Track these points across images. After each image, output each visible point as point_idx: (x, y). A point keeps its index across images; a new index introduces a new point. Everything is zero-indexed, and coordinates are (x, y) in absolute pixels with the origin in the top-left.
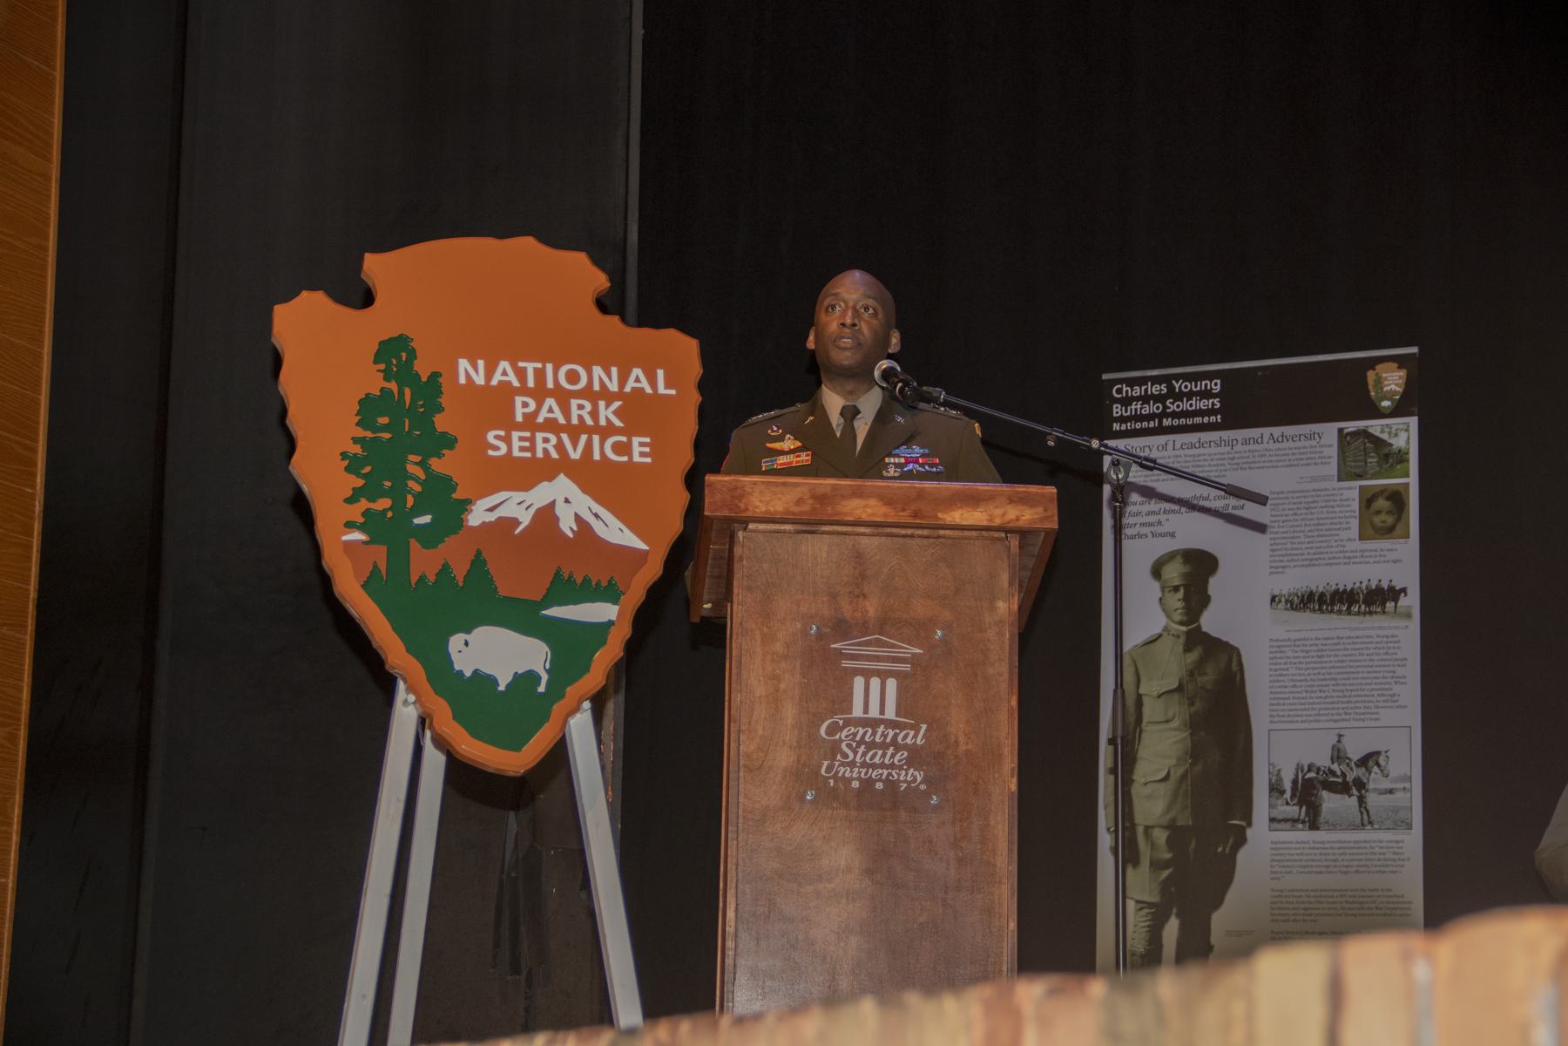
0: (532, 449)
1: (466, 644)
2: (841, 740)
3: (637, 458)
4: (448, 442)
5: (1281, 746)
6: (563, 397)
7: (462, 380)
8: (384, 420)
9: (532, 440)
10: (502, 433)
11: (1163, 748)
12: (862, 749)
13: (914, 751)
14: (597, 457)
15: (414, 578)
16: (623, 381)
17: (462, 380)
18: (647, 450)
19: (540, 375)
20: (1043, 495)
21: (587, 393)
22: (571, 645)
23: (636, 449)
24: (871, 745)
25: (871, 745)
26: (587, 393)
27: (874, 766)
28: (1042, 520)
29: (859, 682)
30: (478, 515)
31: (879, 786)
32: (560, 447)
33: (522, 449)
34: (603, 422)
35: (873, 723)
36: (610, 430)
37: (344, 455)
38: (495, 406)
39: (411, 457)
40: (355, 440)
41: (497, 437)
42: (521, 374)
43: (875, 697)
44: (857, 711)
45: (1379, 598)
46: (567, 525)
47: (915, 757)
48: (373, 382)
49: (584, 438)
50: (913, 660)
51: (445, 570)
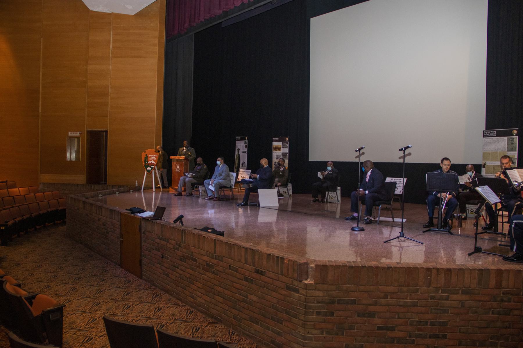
5: (241, 162)
11: (237, 161)
22: (152, 168)
43: (178, 167)
45: (245, 152)
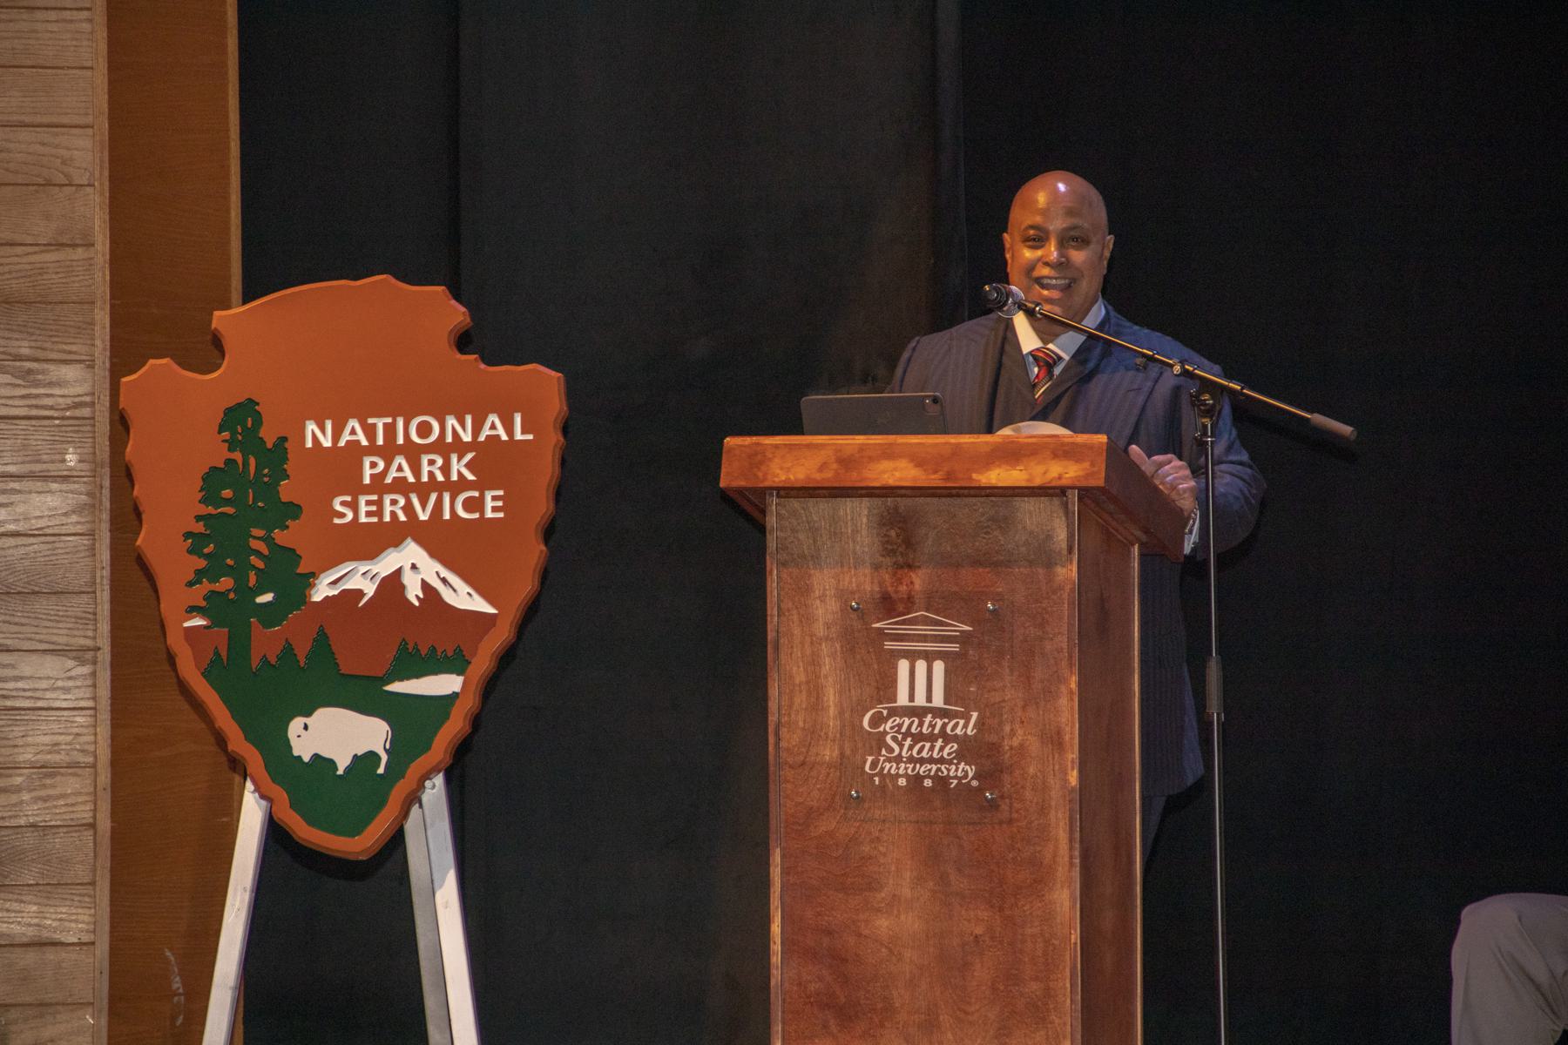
0: (379, 513)
1: (306, 727)
2: (885, 733)
3: (489, 514)
4: (294, 510)
6: (413, 454)
7: (309, 444)
8: (227, 493)
9: (380, 503)
10: (348, 498)
12: (909, 741)
13: (963, 741)
14: (447, 516)
15: (255, 663)
16: (476, 431)
17: (309, 444)
18: (500, 504)
19: (390, 430)
20: (1090, 447)
21: (440, 447)
22: (411, 721)
23: (489, 504)
24: (918, 738)
25: (918, 738)
26: (440, 447)
27: (922, 761)
28: (1087, 476)
29: (903, 666)
30: (322, 591)
31: (928, 783)
32: (408, 509)
33: (369, 514)
34: (455, 477)
35: (919, 713)
36: (462, 484)
37: (188, 535)
38: (341, 468)
39: (256, 532)
40: (199, 518)
41: (343, 503)
42: (370, 431)
43: (920, 682)
44: (902, 699)
46: (413, 593)
47: (967, 750)
48: (216, 452)
49: (433, 497)
50: (964, 639)
51: (288, 651)
